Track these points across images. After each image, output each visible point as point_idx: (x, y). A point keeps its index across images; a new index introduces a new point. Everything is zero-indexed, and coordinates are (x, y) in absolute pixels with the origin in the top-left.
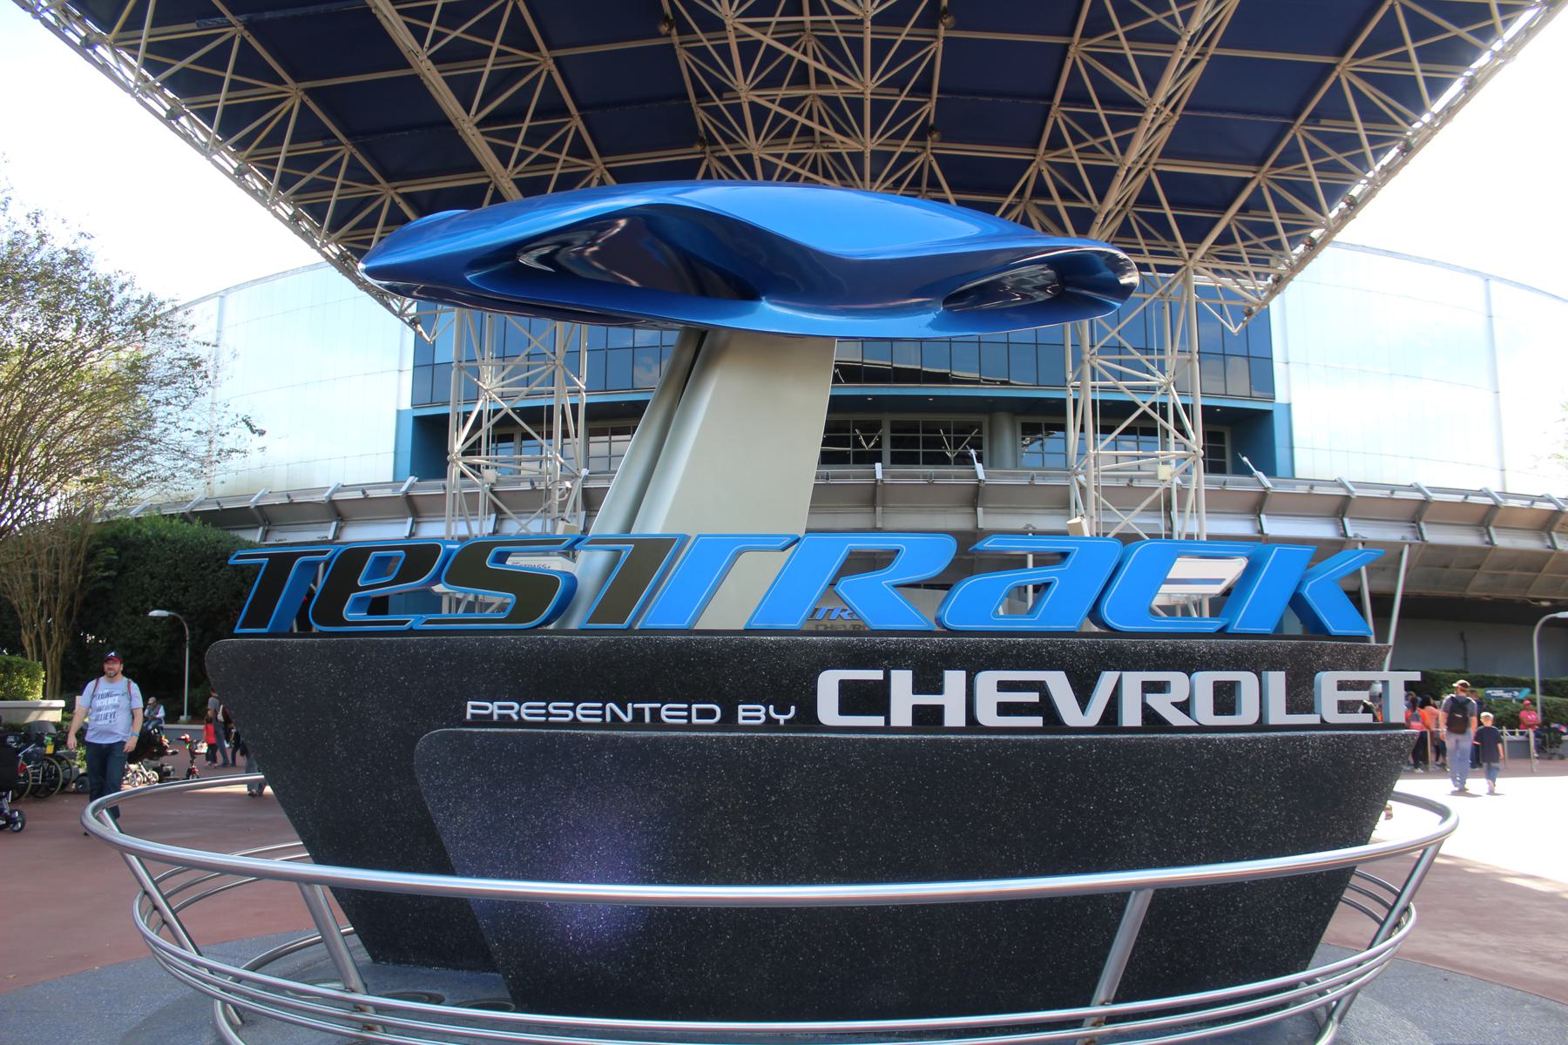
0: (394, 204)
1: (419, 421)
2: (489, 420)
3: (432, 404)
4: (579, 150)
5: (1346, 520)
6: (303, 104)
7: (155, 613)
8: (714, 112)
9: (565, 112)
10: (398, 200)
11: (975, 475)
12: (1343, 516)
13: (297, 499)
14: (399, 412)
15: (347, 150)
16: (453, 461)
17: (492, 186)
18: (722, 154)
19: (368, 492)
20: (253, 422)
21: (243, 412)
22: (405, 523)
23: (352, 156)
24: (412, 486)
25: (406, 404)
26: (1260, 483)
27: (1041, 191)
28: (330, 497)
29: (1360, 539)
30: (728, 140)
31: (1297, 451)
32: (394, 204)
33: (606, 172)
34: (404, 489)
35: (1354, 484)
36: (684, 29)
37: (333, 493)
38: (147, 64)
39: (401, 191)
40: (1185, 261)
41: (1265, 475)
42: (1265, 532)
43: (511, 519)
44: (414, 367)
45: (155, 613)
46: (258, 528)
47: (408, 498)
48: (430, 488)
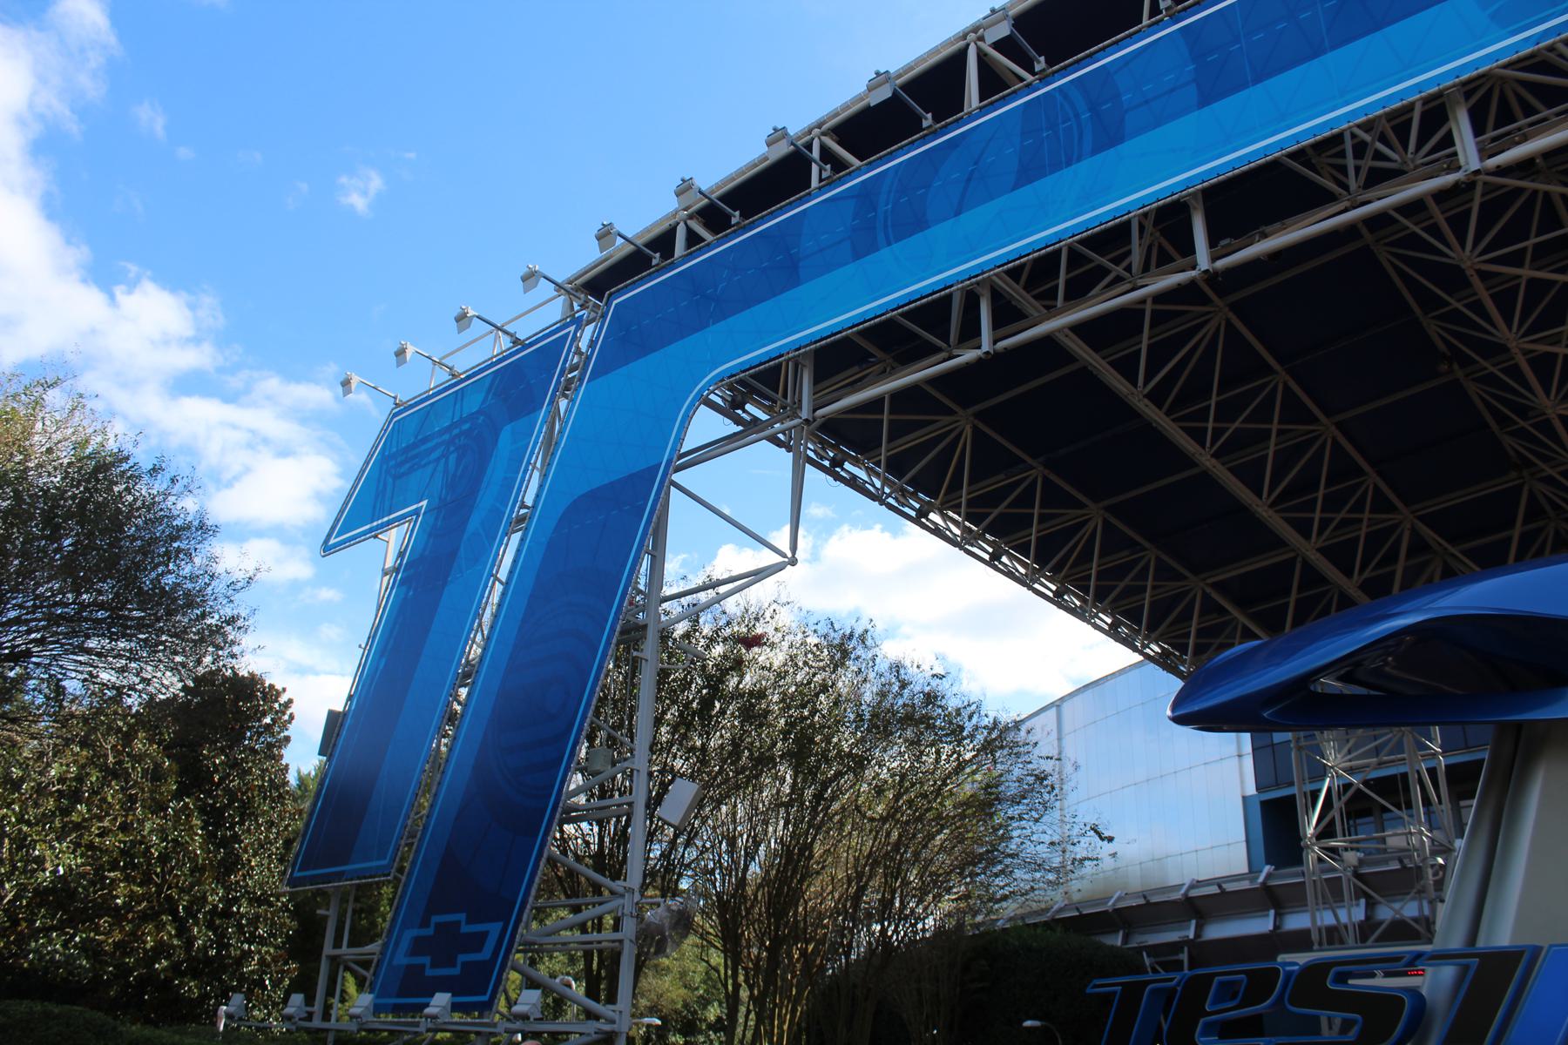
0: (1205, 596)
2: (1340, 799)
3: (1277, 785)
4: (1382, 505)
6: (1105, 522)
7: (1028, 1023)
8: (1521, 434)
9: (1360, 472)
10: (1208, 590)
13: (1154, 899)
14: (1244, 798)
15: (1151, 554)
16: (1308, 847)
17: (1299, 559)
18: (1544, 474)
19: (1224, 886)
20: (1101, 829)
21: (1091, 820)
22: (1267, 915)
23: (1158, 559)
24: (1269, 876)
25: (1251, 789)
28: (1186, 895)
30: (1545, 459)
32: (1205, 596)
33: (1416, 521)
34: (1261, 879)
36: (1465, 362)
37: (1188, 890)
38: (968, 518)
39: (1209, 581)
43: (1380, 903)
44: (1253, 750)
45: (1028, 1023)
46: (1118, 931)
47: (1265, 887)
48: (1287, 878)
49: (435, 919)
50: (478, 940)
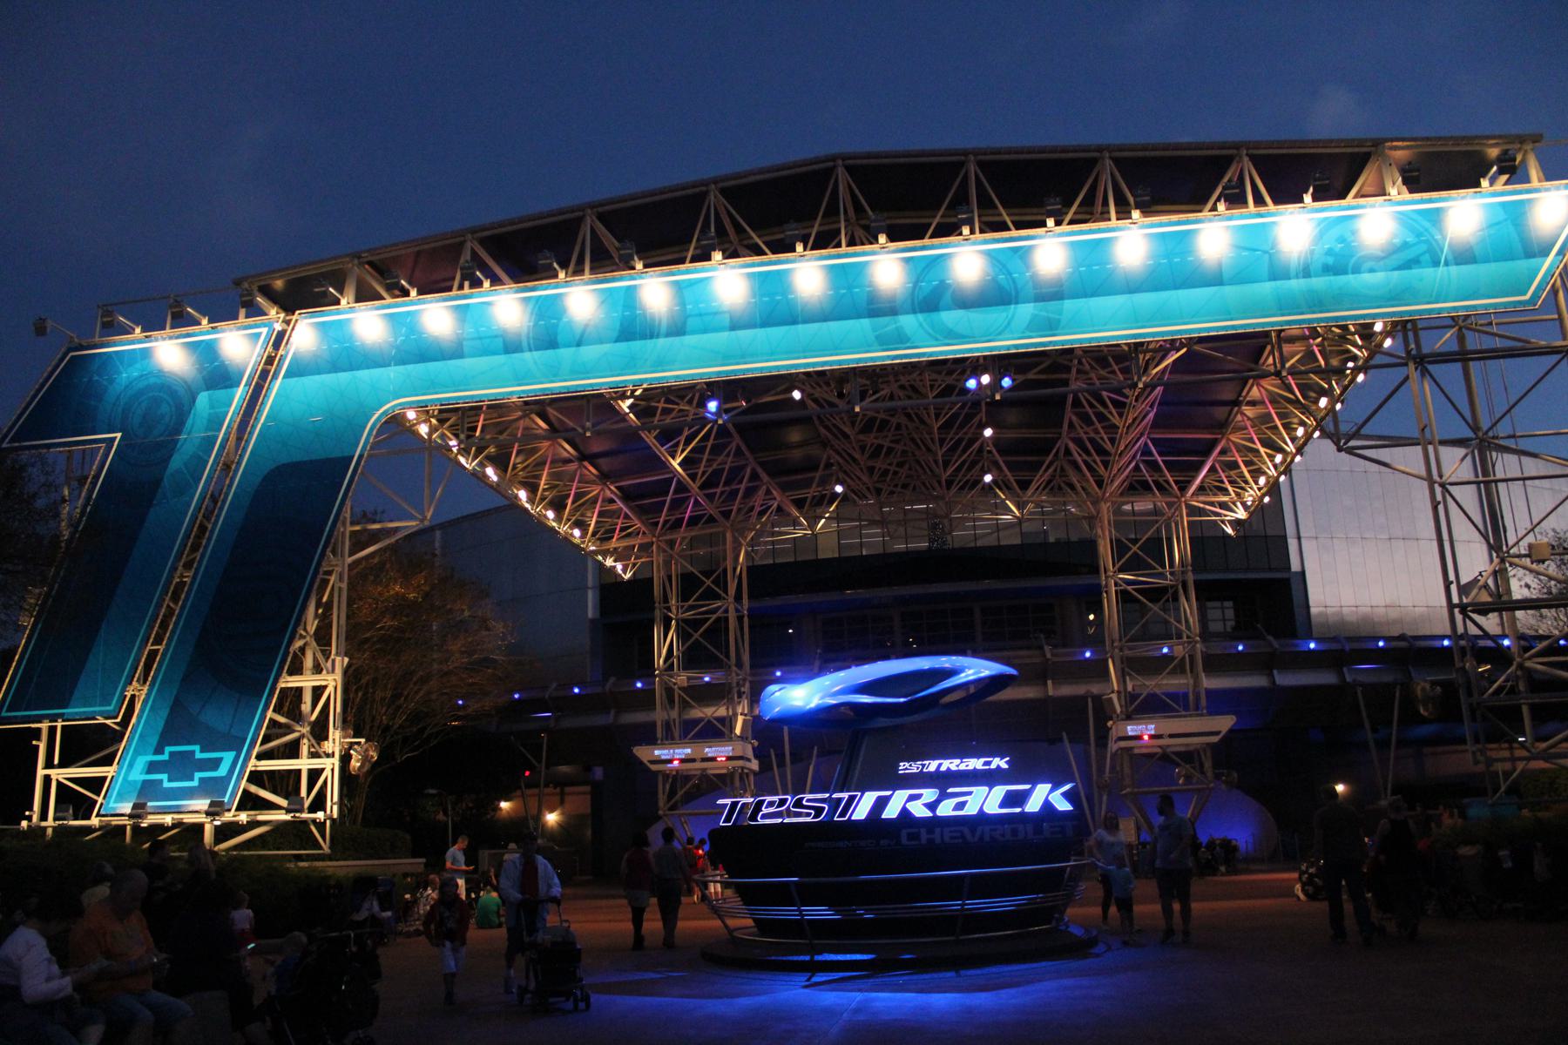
26: (1271, 645)
27: (1068, 452)
40: (1177, 497)
41: (1276, 637)
49: (168, 749)
50: (216, 764)
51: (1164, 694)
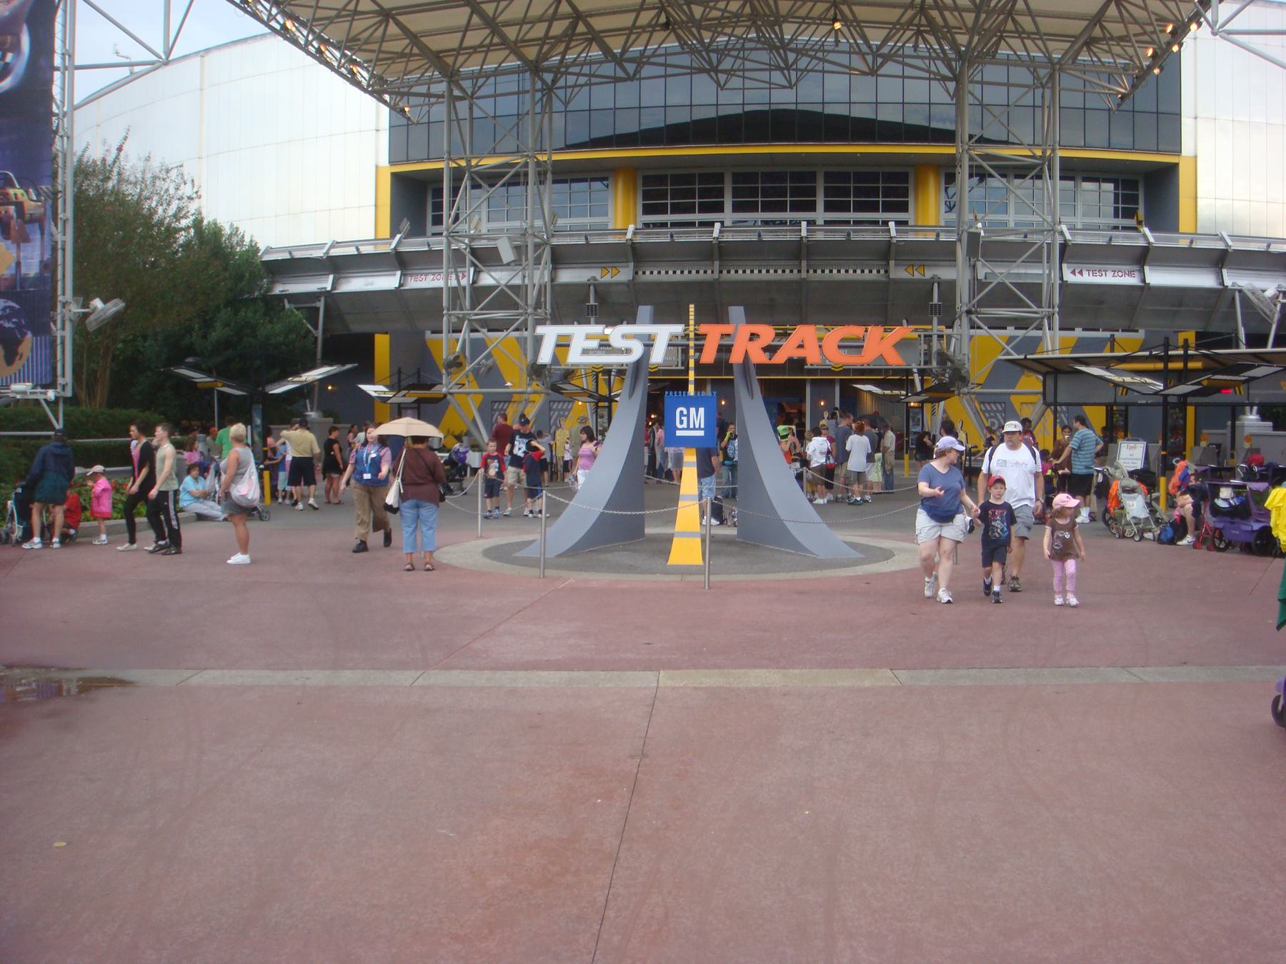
1: (395, 176)
3: (408, 161)
5: (1225, 271)
11: (889, 231)
12: (1222, 267)
13: (298, 255)
22: (395, 275)
26: (1145, 236)
28: (327, 252)
29: (1236, 287)
31: (1199, 200)
34: (393, 246)
35: (1234, 237)
37: (329, 249)
41: (1152, 230)
42: (1147, 282)
44: (390, 127)
51: (1015, 284)
